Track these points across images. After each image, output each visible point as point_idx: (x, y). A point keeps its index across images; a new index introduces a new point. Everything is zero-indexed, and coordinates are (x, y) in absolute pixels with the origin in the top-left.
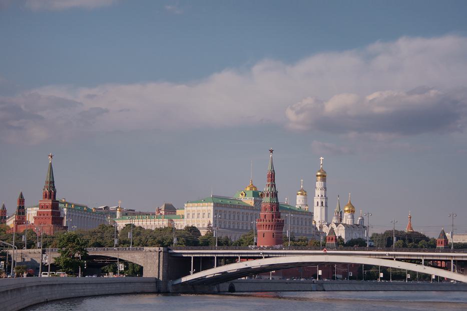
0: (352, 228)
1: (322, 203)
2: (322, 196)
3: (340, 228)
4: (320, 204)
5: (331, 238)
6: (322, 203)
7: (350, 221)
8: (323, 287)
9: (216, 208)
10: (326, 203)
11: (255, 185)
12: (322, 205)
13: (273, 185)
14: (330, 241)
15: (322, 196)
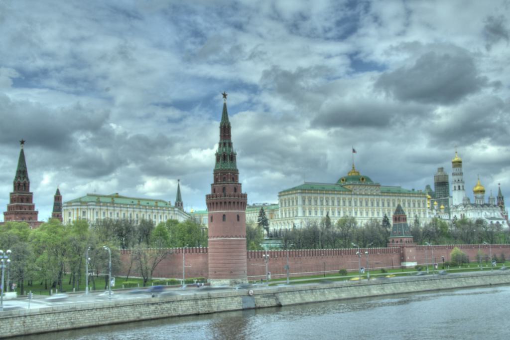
0: (481, 208)
1: (459, 187)
2: (459, 181)
3: (469, 209)
4: (457, 188)
5: (398, 217)
6: (459, 187)
7: (479, 201)
8: (277, 299)
9: (304, 195)
10: (463, 186)
11: (357, 169)
12: (459, 189)
13: (230, 145)
14: (397, 221)
15: (459, 181)
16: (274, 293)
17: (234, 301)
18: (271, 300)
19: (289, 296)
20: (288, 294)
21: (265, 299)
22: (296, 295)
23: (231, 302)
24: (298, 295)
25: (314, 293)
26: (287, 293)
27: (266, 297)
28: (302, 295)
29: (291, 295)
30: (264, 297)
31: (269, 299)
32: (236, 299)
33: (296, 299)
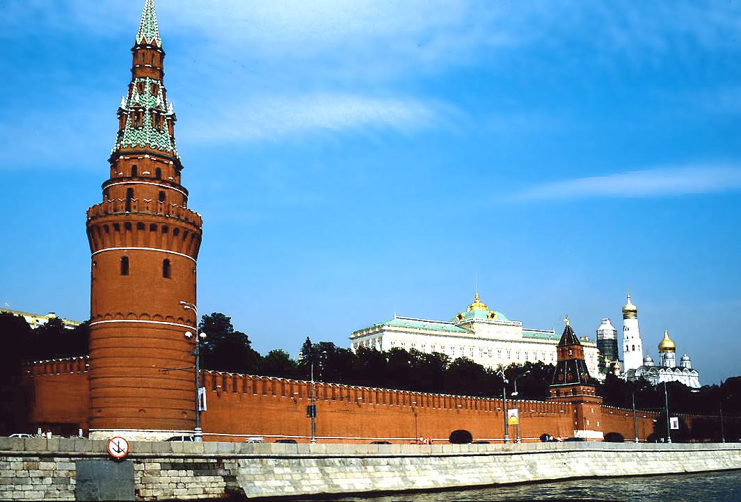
8: (230, 478)
16: (220, 459)
17: (34, 473)
18: (204, 479)
19: (277, 470)
20: (276, 466)
21: (183, 473)
22: (308, 470)
23: (21, 474)
24: (313, 469)
25: (370, 468)
26: (271, 462)
27: (186, 467)
28: (328, 470)
29: (288, 470)
30: (175, 466)
31: (195, 475)
32: (43, 465)
33: (303, 482)
